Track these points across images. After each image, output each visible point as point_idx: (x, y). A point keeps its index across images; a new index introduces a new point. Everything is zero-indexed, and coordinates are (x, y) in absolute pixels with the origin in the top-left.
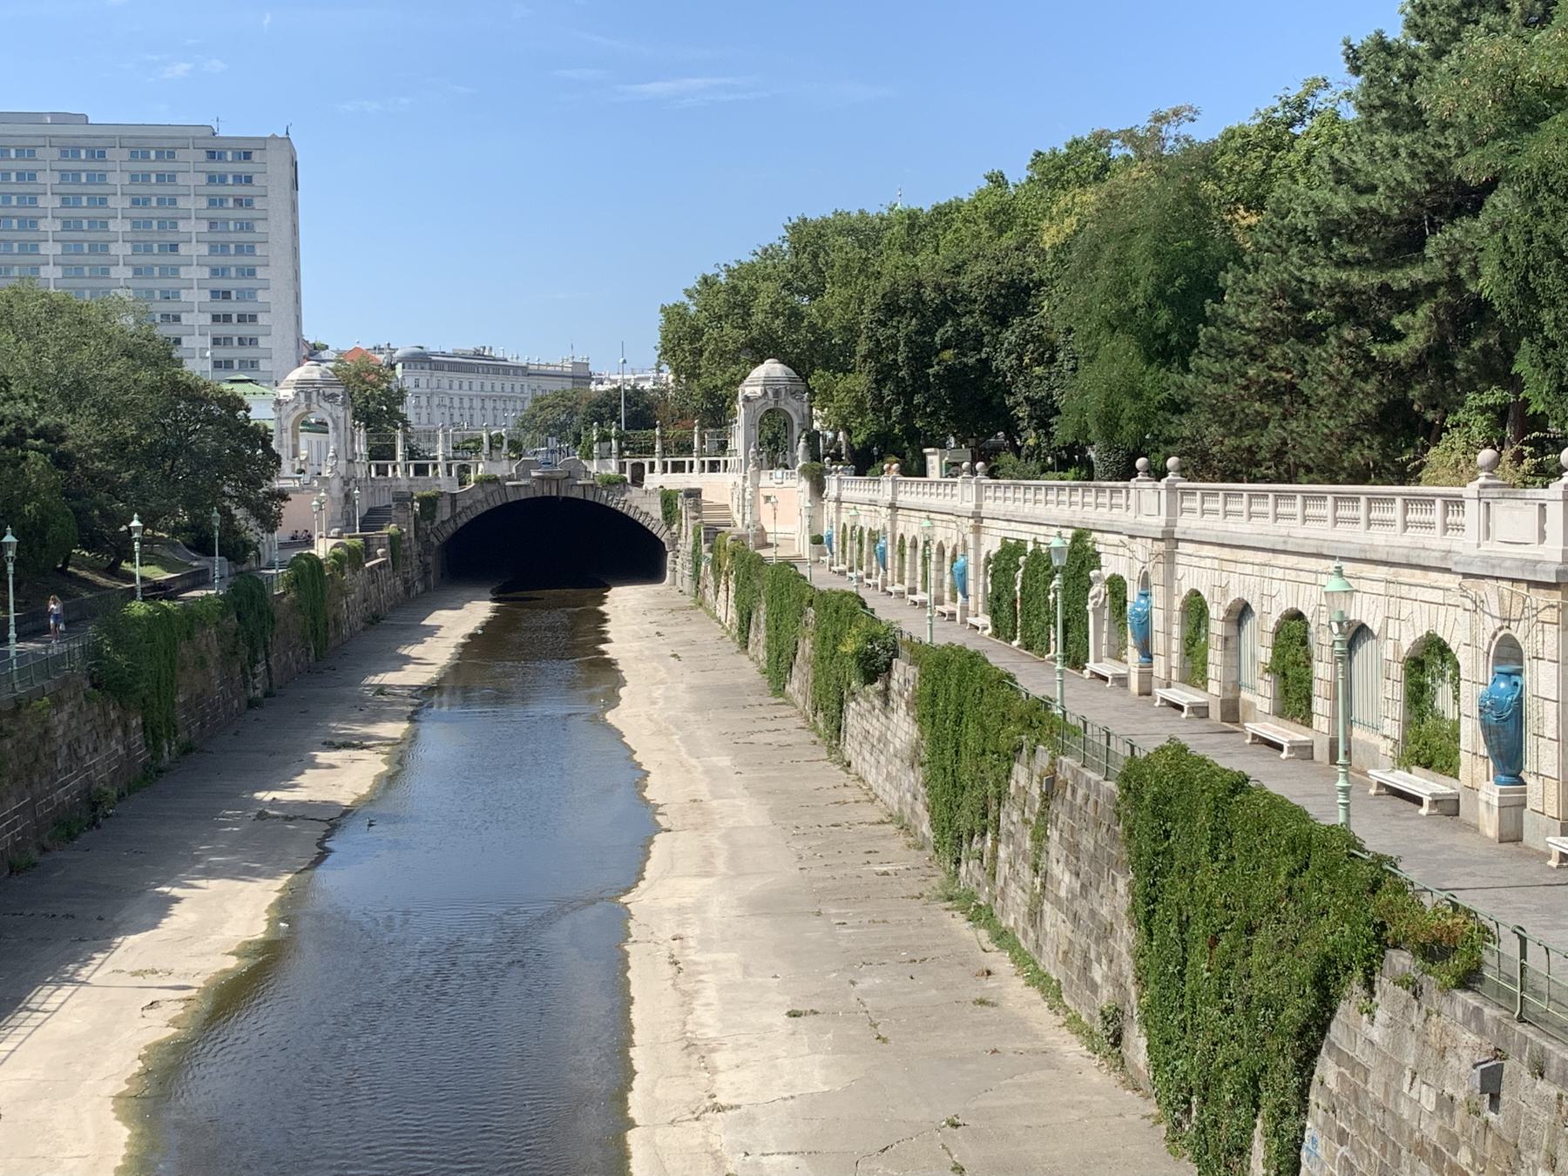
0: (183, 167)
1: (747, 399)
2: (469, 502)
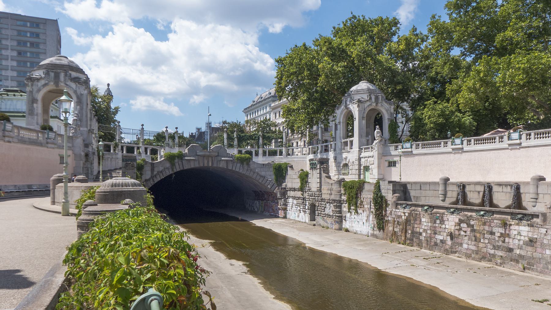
0: (6, 26)
2: (161, 168)
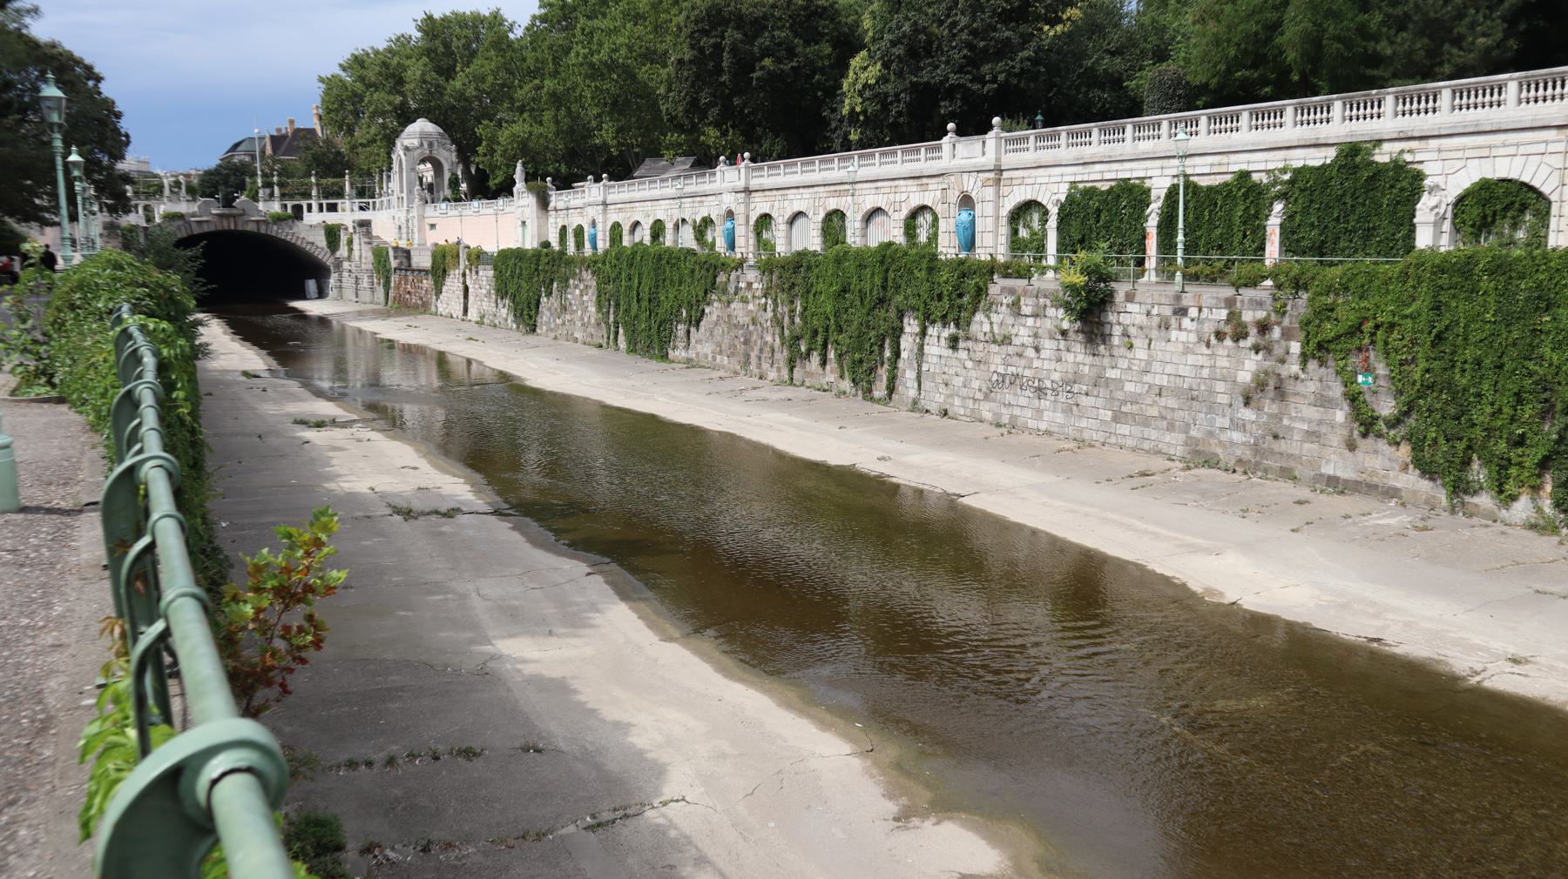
1: (407, 149)
